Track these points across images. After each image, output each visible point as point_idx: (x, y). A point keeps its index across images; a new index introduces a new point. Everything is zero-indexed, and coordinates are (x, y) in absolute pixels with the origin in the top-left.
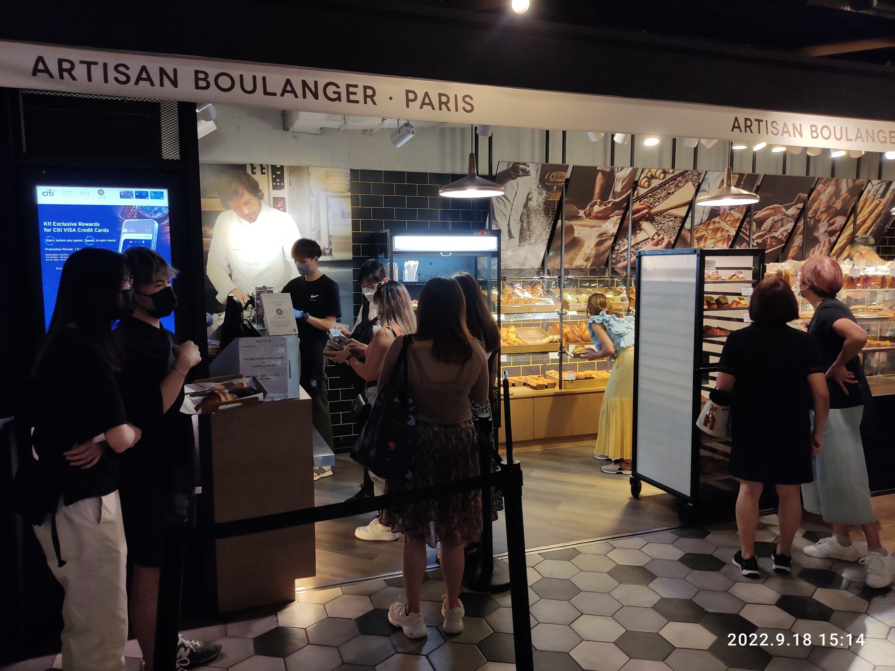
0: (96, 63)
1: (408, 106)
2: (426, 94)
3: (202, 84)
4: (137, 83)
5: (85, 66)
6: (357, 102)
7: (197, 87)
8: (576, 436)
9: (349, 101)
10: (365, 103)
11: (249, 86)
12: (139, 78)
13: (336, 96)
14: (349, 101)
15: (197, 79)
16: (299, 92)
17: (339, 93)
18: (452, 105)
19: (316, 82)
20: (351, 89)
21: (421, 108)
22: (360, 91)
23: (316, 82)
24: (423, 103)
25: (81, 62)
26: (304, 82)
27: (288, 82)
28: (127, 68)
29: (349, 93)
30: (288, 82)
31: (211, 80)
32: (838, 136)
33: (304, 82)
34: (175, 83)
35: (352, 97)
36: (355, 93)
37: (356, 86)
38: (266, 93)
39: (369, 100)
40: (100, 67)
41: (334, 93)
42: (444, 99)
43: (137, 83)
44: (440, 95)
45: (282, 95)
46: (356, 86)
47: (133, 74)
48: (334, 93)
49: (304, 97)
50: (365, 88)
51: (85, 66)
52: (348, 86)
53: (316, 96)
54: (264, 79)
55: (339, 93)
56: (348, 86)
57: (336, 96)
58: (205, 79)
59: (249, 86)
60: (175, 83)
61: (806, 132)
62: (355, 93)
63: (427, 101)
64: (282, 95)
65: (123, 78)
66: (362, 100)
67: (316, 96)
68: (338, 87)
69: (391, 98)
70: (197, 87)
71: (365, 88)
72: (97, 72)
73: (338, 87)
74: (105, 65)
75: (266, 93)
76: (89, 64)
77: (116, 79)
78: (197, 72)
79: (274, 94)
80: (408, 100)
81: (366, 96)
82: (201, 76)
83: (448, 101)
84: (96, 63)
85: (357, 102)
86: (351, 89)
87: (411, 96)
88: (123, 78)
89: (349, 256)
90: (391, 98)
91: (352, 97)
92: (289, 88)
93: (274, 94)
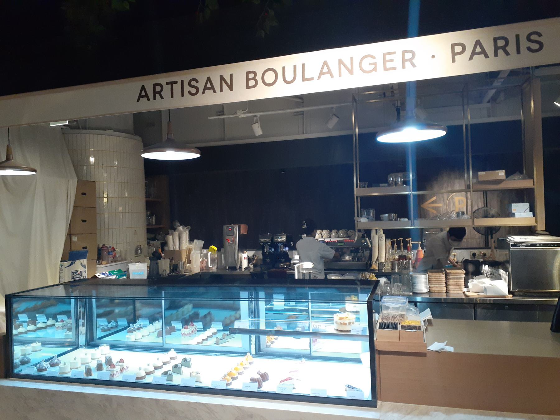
0: (176, 82)
1: (454, 60)
2: (478, 43)
4: (203, 93)
5: (170, 85)
6: (394, 68)
7: (248, 87)
8: (136, 285)
9: (385, 69)
10: (404, 67)
12: (205, 89)
13: (373, 66)
14: (385, 69)
15: (248, 80)
17: (375, 64)
18: (511, 48)
20: (388, 57)
21: (471, 58)
22: (398, 58)
24: (474, 53)
25: (167, 83)
28: (197, 81)
29: (385, 61)
35: (389, 65)
36: (392, 60)
37: (394, 53)
39: (408, 64)
41: (371, 64)
43: (203, 93)
45: (319, 78)
46: (394, 53)
48: (371, 64)
51: (170, 85)
52: (385, 55)
53: (351, 72)
55: (375, 64)
56: (385, 55)
57: (373, 66)
58: (254, 79)
62: (392, 60)
65: (194, 91)
67: (351, 72)
68: (374, 57)
69: (433, 57)
70: (248, 87)
71: (404, 52)
73: (374, 57)
74: (182, 82)
76: (172, 84)
77: (189, 92)
80: (454, 54)
81: (404, 61)
84: (176, 82)
85: (394, 68)
86: (388, 57)
88: (194, 91)
89: (443, 277)
90: (433, 57)
91: (389, 65)
92: (325, 70)
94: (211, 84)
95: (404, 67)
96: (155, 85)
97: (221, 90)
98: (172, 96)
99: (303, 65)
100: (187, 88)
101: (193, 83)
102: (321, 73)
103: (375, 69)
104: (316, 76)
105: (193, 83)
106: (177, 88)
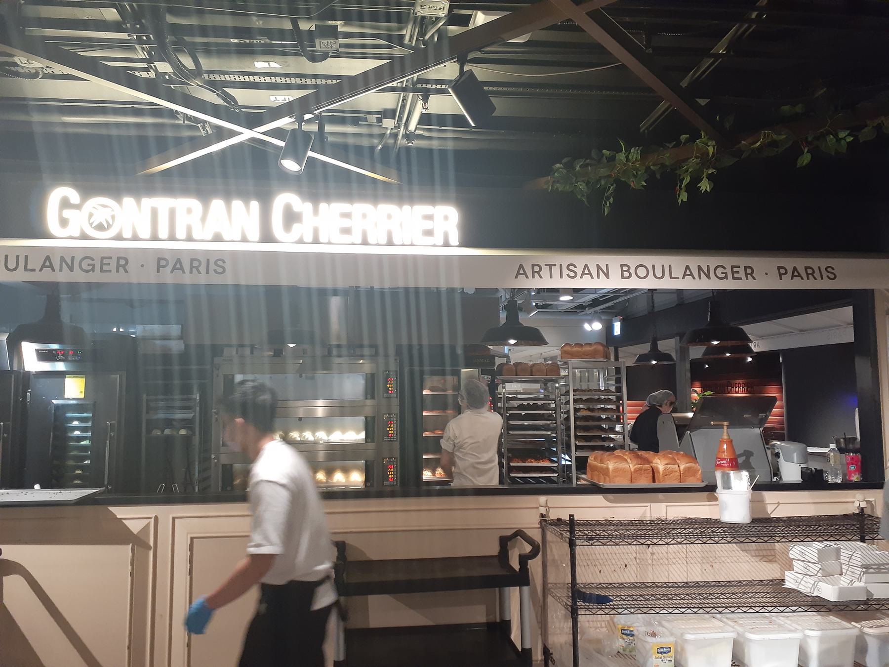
0: (555, 265)
3: (626, 274)
6: (741, 279)
7: (623, 277)
9: (734, 278)
10: (747, 278)
11: (659, 274)
12: (583, 274)
14: (734, 278)
15: (623, 271)
16: (594, 274)
17: (726, 273)
19: (708, 266)
20: (735, 270)
23: (708, 266)
26: (699, 267)
27: (687, 267)
28: (575, 267)
30: (687, 267)
31: (632, 271)
32: (659, 274)
33: (699, 267)
34: (607, 275)
35: (736, 275)
37: (739, 267)
38: (671, 278)
40: (558, 266)
42: (810, 271)
44: (806, 268)
46: (739, 267)
47: (579, 271)
49: (598, 277)
50: (746, 268)
52: (732, 267)
54: (670, 266)
55: (726, 273)
58: (628, 271)
59: (659, 273)
60: (607, 275)
61: (615, 272)
63: (795, 273)
64: (683, 278)
66: (744, 277)
67: (708, 277)
68: (725, 268)
70: (623, 277)
71: (746, 268)
72: (556, 270)
73: (725, 268)
75: (671, 278)
78: (622, 266)
79: (678, 278)
82: (625, 268)
83: (814, 272)
84: (555, 265)
85: (741, 279)
86: (735, 270)
87: (782, 271)
88: (572, 274)
91: (736, 275)
93: (678, 278)
94: (589, 270)
95: (747, 278)
96: (533, 266)
97: (598, 277)
98: (551, 277)
99: (670, 266)
100: (565, 272)
101: (571, 268)
102: (685, 275)
103: (726, 277)
104: (681, 277)
105: (571, 268)
106: (556, 270)
